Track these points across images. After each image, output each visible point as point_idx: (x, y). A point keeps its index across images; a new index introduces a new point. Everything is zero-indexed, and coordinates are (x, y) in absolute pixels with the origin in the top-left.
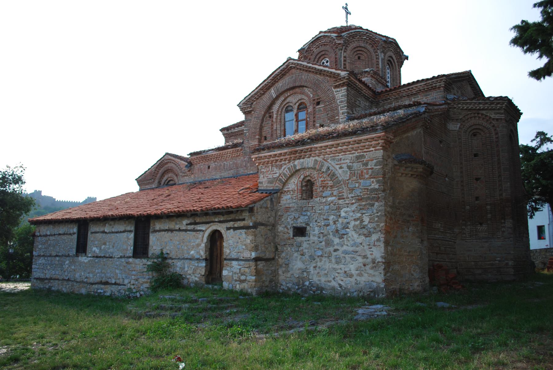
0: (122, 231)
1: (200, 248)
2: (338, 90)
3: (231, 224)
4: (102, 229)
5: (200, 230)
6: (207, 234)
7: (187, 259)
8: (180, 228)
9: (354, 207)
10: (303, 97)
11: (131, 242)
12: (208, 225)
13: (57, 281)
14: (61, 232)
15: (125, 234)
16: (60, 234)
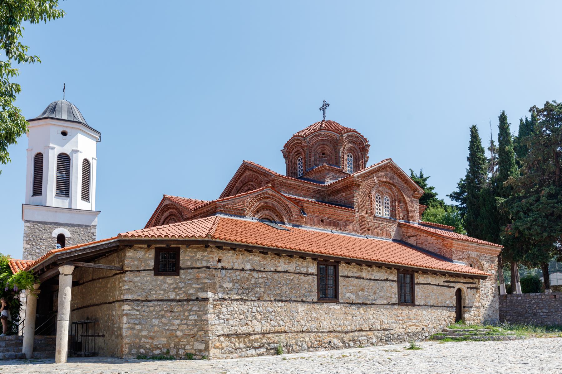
0: (383, 279)
1: (453, 299)
2: (415, 199)
3: (469, 285)
4: (357, 274)
5: (453, 287)
6: (456, 289)
7: (445, 307)
8: (439, 284)
9: (490, 282)
10: (390, 192)
11: (396, 290)
12: (457, 284)
13: (283, 335)
14: (279, 269)
15: (388, 283)
16: (276, 271)
